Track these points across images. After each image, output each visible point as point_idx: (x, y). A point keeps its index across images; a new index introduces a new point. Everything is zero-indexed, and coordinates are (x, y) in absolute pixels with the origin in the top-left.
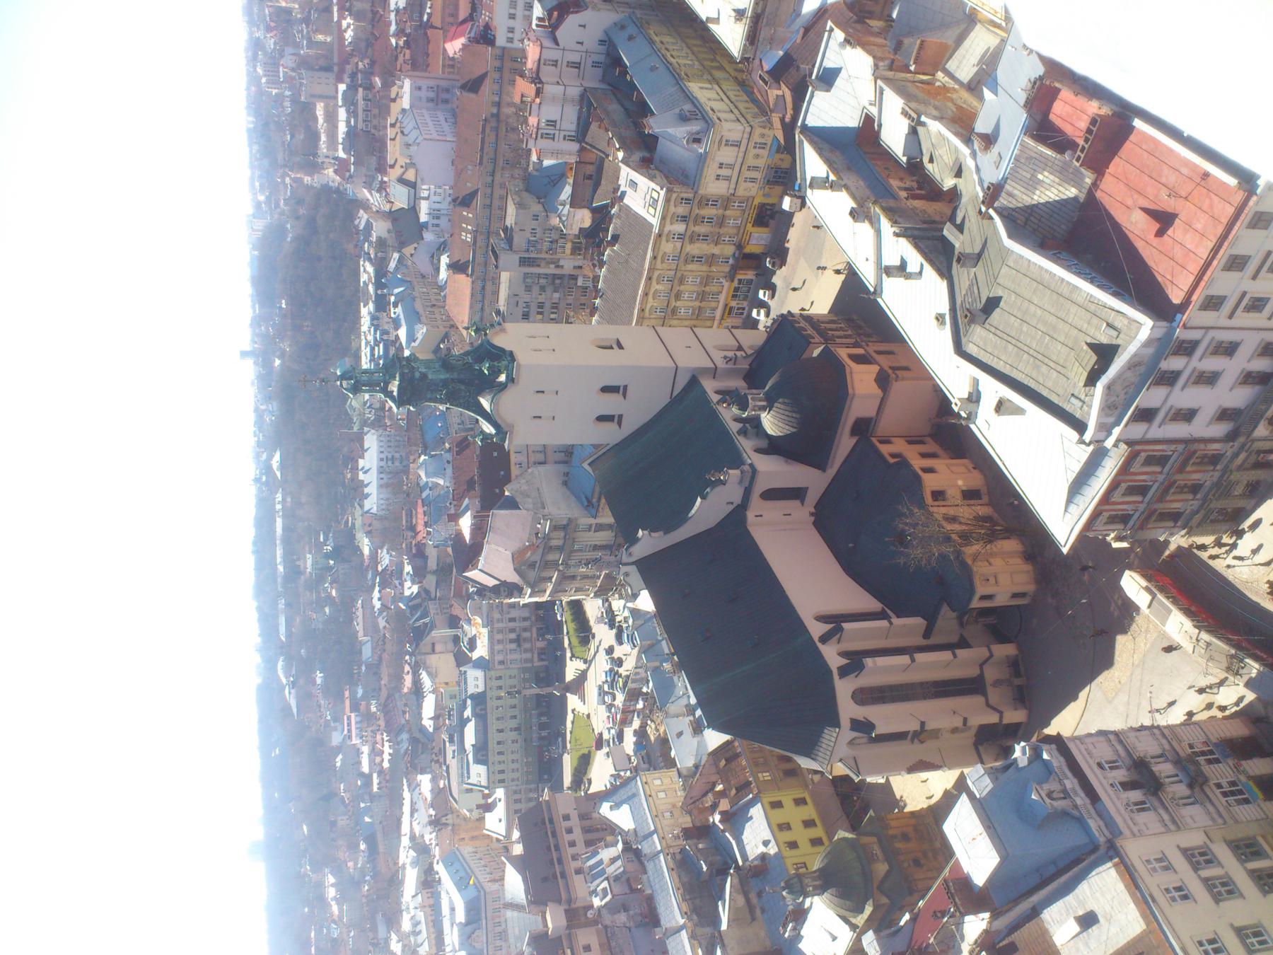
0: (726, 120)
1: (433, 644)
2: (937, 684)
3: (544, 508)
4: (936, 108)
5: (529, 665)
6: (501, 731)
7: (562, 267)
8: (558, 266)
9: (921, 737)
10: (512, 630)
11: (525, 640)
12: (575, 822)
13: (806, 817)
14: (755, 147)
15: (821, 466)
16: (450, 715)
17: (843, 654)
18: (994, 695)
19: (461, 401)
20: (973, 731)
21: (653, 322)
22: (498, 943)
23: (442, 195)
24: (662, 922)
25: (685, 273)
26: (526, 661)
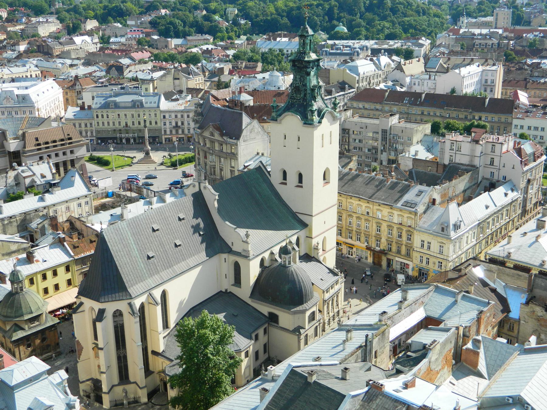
0: (454, 246)
1: (178, 79)
2: (125, 357)
3: (244, 141)
4: (436, 359)
5: (163, 133)
6: (125, 115)
7: (382, 154)
8: (382, 150)
9: (96, 348)
10: (183, 124)
11: (177, 132)
12: (69, 157)
13: (60, 286)
14: (439, 262)
15: (252, 296)
16: (136, 87)
17: (142, 307)
18: (119, 389)
19: (295, 95)
20: (99, 378)
21: (344, 204)
22: (6, 113)
24: (7, 204)
25: (371, 222)
26: (165, 131)
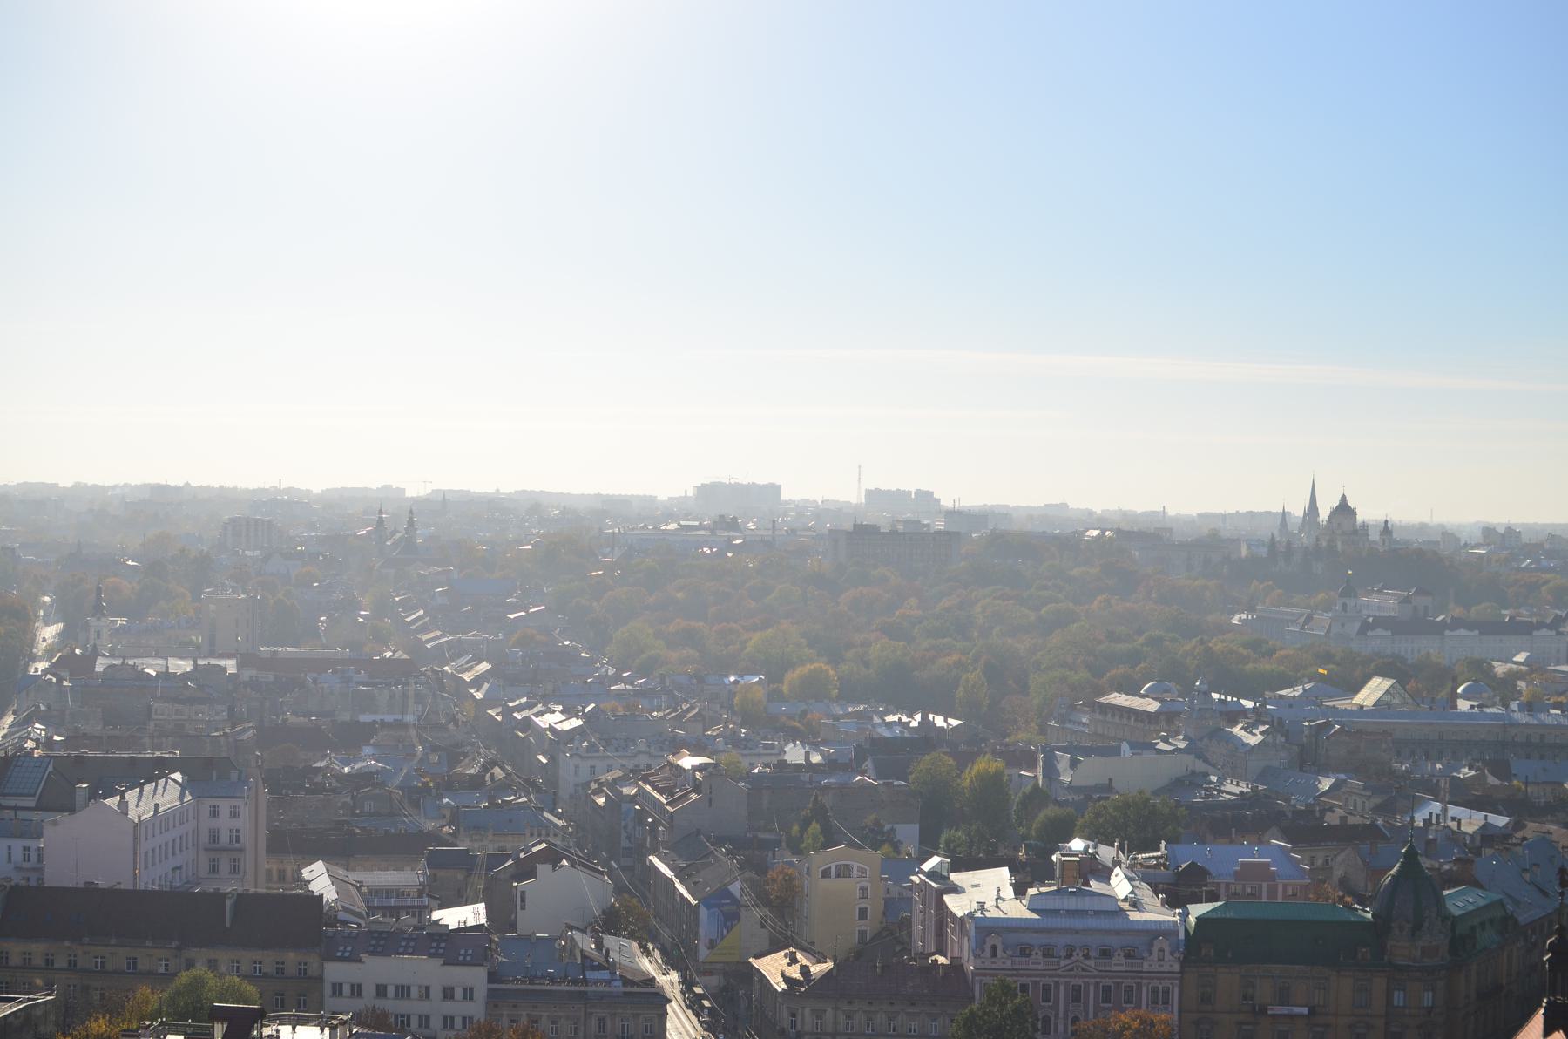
23: (26, 865)
